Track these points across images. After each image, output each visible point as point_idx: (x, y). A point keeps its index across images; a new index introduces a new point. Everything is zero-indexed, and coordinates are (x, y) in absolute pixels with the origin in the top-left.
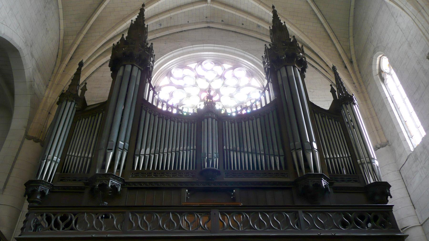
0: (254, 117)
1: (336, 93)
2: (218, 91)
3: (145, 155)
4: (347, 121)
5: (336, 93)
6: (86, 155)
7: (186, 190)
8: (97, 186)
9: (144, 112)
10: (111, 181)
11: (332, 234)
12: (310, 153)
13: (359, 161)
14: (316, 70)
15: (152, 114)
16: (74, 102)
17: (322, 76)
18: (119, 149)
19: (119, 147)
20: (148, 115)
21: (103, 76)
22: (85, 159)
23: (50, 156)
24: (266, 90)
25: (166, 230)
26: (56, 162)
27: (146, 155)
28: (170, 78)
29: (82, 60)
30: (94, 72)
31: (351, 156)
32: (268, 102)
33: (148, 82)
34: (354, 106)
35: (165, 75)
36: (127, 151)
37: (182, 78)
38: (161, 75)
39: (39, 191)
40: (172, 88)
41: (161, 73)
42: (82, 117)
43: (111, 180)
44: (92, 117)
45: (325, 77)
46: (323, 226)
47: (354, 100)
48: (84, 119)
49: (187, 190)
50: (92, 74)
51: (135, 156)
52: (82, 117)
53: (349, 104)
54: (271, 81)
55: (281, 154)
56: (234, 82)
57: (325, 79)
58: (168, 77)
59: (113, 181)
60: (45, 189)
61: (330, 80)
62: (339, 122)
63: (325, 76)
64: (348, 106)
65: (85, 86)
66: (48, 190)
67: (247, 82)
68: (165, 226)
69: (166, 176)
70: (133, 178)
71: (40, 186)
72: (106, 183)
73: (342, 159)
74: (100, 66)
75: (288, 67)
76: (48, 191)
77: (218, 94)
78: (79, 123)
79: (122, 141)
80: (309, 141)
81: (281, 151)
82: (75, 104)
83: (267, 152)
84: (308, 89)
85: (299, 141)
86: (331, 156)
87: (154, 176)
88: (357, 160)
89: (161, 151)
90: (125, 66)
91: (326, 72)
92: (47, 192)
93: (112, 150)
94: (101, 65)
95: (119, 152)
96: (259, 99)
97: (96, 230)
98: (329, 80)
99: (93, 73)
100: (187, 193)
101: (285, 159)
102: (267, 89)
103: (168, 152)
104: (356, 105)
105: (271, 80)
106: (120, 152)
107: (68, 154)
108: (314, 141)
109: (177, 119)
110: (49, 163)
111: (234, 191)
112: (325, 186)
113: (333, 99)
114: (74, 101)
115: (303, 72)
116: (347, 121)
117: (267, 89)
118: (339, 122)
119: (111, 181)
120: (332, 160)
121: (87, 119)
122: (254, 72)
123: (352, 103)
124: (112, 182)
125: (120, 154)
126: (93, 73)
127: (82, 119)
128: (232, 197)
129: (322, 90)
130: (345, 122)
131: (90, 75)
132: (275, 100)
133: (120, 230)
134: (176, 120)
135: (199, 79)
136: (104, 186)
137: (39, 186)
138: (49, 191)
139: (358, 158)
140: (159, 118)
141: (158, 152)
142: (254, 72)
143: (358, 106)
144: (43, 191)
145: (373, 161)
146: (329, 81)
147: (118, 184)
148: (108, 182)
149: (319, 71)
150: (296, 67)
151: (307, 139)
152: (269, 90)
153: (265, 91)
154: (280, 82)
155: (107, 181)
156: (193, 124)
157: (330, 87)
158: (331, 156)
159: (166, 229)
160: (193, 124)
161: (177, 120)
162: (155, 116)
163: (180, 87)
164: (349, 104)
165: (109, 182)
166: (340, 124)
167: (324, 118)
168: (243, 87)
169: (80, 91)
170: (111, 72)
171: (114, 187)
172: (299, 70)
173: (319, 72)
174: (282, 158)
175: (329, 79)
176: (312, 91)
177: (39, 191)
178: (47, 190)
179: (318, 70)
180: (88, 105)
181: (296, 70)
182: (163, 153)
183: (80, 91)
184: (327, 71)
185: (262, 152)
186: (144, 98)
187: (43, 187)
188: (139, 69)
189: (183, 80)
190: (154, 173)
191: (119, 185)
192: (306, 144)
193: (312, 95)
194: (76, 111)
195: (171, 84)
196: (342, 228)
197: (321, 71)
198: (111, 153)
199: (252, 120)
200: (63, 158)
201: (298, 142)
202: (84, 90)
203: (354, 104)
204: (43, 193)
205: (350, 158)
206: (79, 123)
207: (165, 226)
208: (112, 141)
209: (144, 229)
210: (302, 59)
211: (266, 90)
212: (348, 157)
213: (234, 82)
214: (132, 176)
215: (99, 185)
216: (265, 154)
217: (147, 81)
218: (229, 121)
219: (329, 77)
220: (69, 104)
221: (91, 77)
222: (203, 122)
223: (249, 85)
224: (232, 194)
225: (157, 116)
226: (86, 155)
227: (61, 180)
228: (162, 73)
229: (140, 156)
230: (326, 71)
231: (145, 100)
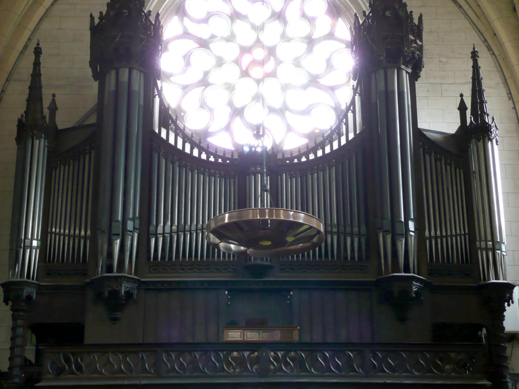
0: (326, 165)
1: (468, 112)
2: (272, 51)
3: (163, 234)
4: (474, 170)
5: (468, 112)
6: (77, 232)
7: (225, 292)
8: (107, 294)
9: (156, 156)
10: (124, 286)
11: (400, 381)
12: (402, 240)
13: (478, 243)
14: (459, 8)
15: (169, 159)
16: (43, 138)
17: (469, 25)
18: (128, 232)
19: (128, 229)
20: (163, 161)
21: (60, 29)
22: (77, 239)
23: (27, 242)
24: (350, 111)
25: (207, 373)
26: (36, 248)
27: (166, 235)
28: (182, 20)
29: (37, 42)
30: (42, 17)
31: (469, 234)
32: (351, 136)
33: (156, 95)
34: (490, 144)
35: (174, 12)
36: (138, 231)
37: (206, 21)
38: (166, 16)
39: (24, 296)
40: (191, 44)
41: (166, 11)
42: (59, 162)
43: (123, 285)
44: (74, 163)
45: (474, 29)
46: (392, 369)
47: (491, 132)
48: (62, 165)
49: (227, 292)
50: (39, 22)
51: (150, 236)
52: (59, 162)
53: (482, 141)
54: (360, 91)
55: (362, 233)
56: (304, 28)
57: (474, 31)
58: (179, 18)
59: (126, 285)
60: (31, 292)
61: (481, 34)
62: (462, 170)
63: (474, 23)
64: (481, 144)
65: (53, 102)
66: (35, 292)
67: (326, 31)
68: (206, 369)
69: (197, 269)
70: (151, 273)
71: (25, 290)
72: (117, 288)
73: (454, 238)
74: (52, 4)
75: (389, 71)
76: (35, 293)
77: (272, 58)
78: (56, 173)
79: (130, 219)
80: (403, 220)
81: (363, 230)
82: (45, 139)
83: (342, 229)
84: (438, 56)
85: (390, 219)
86: (438, 233)
87: (180, 271)
88: (476, 241)
89: (187, 228)
90: (117, 70)
91: (477, 18)
92: (34, 296)
93: (119, 235)
94: (53, 2)
95: (128, 237)
96: (337, 131)
97: (124, 373)
98: (480, 35)
99: (41, 20)
100: (227, 297)
101: (368, 241)
102: (352, 108)
103: (197, 229)
104: (494, 141)
105: (359, 89)
106: (130, 237)
107: (49, 230)
108: (412, 217)
109: (207, 170)
110: (28, 250)
111: (291, 293)
112: (416, 292)
113: (460, 124)
114: (43, 136)
115: (414, 77)
116: (474, 170)
117: (351, 110)
118: (462, 170)
119: (124, 286)
120: (439, 240)
121: (67, 167)
122: (342, 6)
123: (487, 138)
124: (125, 287)
125: (129, 240)
126: (42, 21)
127: (59, 166)
128: (288, 302)
129: (462, 58)
130: (471, 171)
131: (37, 25)
132: (362, 132)
133: (152, 374)
134: (206, 171)
135: (238, 22)
136: (115, 294)
137: (23, 290)
138: (36, 293)
139: (478, 239)
140: (179, 166)
141: (183, 230)
142: (342, 6)
143: (497, 142)
144: (29, 295)
145: (497, 246)
146: (479, 36)
147: (133, 288)
148: (120, 287)
149: (465, 13)
150: (402, 69)
151: (400, 217)
152: (354, 112)
153: (348, 113)
154: (373, 100)
155: (119, 286)
156: (232, 180)
157: (460, 98)
158: (438, 233)
159: (207, 372)
160: (232, 180)
161: (208, 173)
162: (173, 163)
163: (204, 44)
164: (482, 141)
165: (121, 287)
166: (462, 174)
167: (439, 163)
168: (319, 40)
169: (46, 112)
170: (92, 74)
171: (129, 294)
172: (407, 72)
173: (465, 16)
174: (363, 240)
175: (479, 31)
176: (444, 60)
177: (24, 296)
178: (34, 292)
179: (464, 10)
180: (60, 127)
181: (402, 75)
182: (190, 231)
183: (46, 112)
184: (479, 16)
185: (335, 230)
186: (153, 130)
187: (29, 290)
188: (141, 71)
189: (208, 24)
190: (180, 265)
191: (134, 288)
192: (397, 225)
193: (443, 71)
194: (48, 152)
195: (186, 35)
196: (415, 372)
197: (468, 12)
198: (118, 241)
199: (324, 171)
200: (43, 240)
201: (387, 224)
202: (53, 108)
203: (491, 140)
204: (29, 298)
205: (467, 236)
206: (56, 173)
207: (206, 369)
208: (118, 221)
209: (181, 372)
210: (414, 58)
211: (350, 111)
212: (465, 235)
213: (304, 28)
214: (148, 270)
215: (109, 293)
216: (338, 234)
217: (154, 93)
218: (288, 173)
219: (479, 28)
220: (37, 142)
221: (38, 29)
222: (248, 178)
223: (331, 36)
224: (289, 297)
225: (177, 164)
226: (77, 232)
227: (48, 274)
228: (169, 11)
229: (156, 235)
230: (477, 16)
231: (156, 132)
